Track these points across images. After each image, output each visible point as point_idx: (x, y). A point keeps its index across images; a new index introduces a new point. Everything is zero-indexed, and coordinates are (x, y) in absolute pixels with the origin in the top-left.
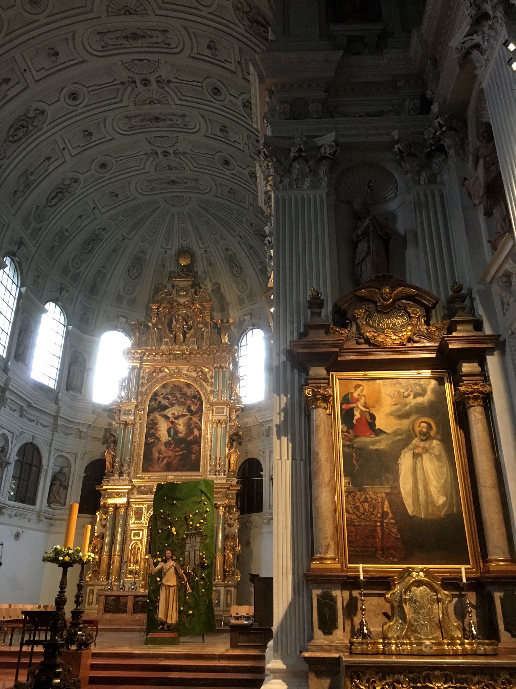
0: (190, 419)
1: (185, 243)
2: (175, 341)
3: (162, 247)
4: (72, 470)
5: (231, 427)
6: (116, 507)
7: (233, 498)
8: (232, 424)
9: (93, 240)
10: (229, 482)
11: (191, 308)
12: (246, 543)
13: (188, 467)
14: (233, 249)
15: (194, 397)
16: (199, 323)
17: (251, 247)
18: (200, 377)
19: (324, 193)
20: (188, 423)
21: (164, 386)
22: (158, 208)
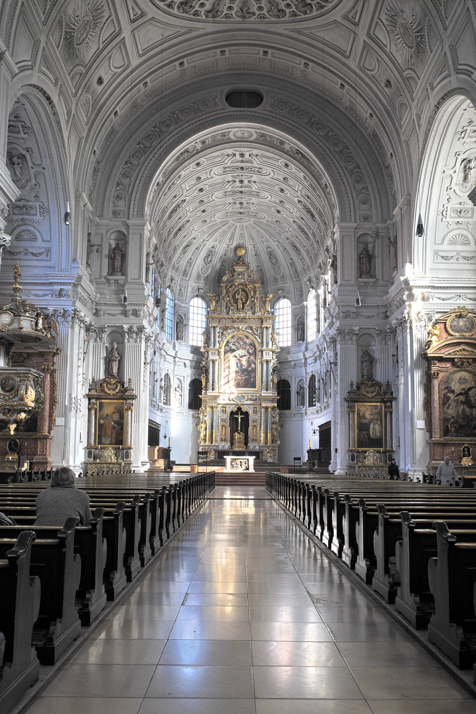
0: (249, 358)
1: (241, 242)
2: (238, 309)
3: (226, 244)
4: (183, 385)
5: (273, 364)
6: (212, 408)
7: (275, 403)
8: (274, 361)
9: (188, 246)
10: (273, 395)
11: (247, 287)
12: (282, 426)
13: (249, 385)
14: (273, 248)
15: (251, 344)
16: (252, 297)
17: (285, 249)
18: (254, 334)
19: (355, 346)
20: (248, 360)
21: (233, 337)
22: (227, 223)
